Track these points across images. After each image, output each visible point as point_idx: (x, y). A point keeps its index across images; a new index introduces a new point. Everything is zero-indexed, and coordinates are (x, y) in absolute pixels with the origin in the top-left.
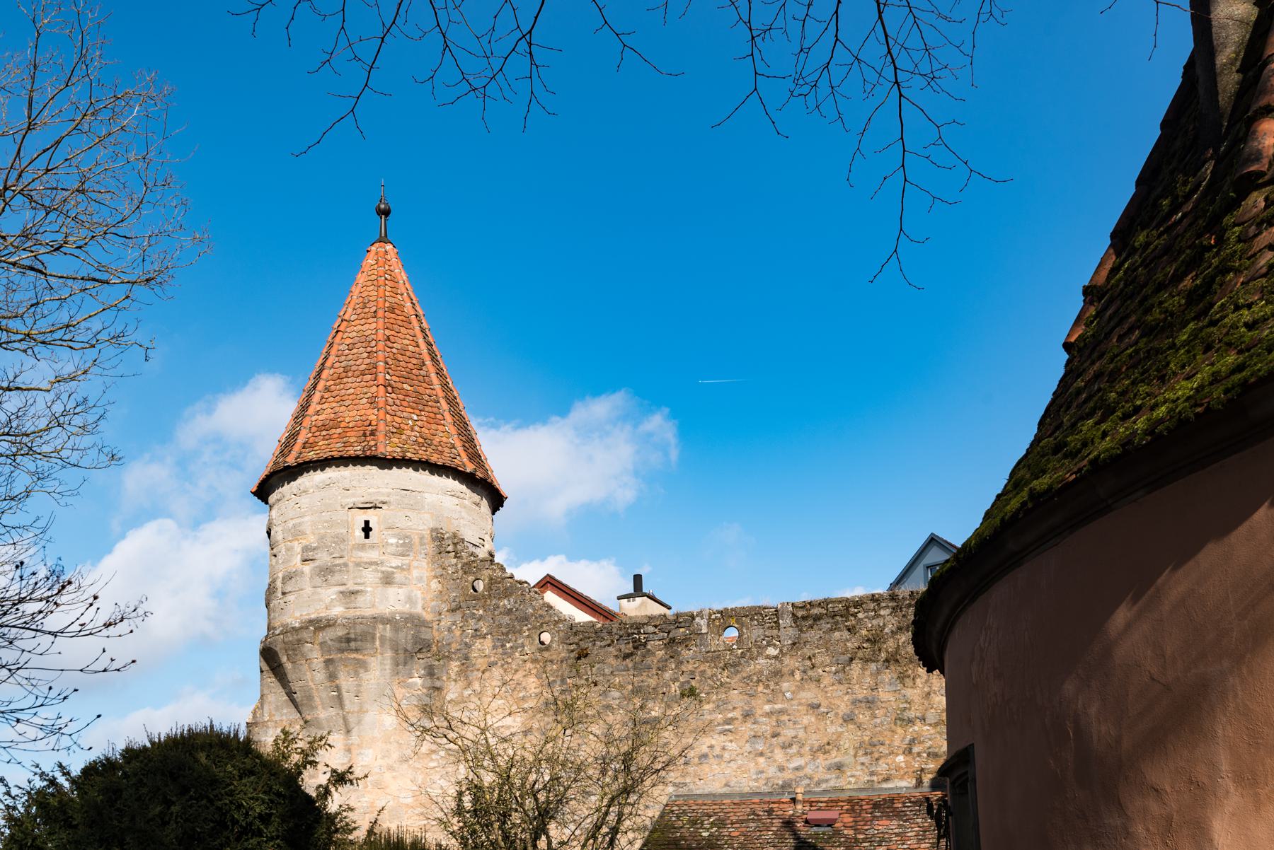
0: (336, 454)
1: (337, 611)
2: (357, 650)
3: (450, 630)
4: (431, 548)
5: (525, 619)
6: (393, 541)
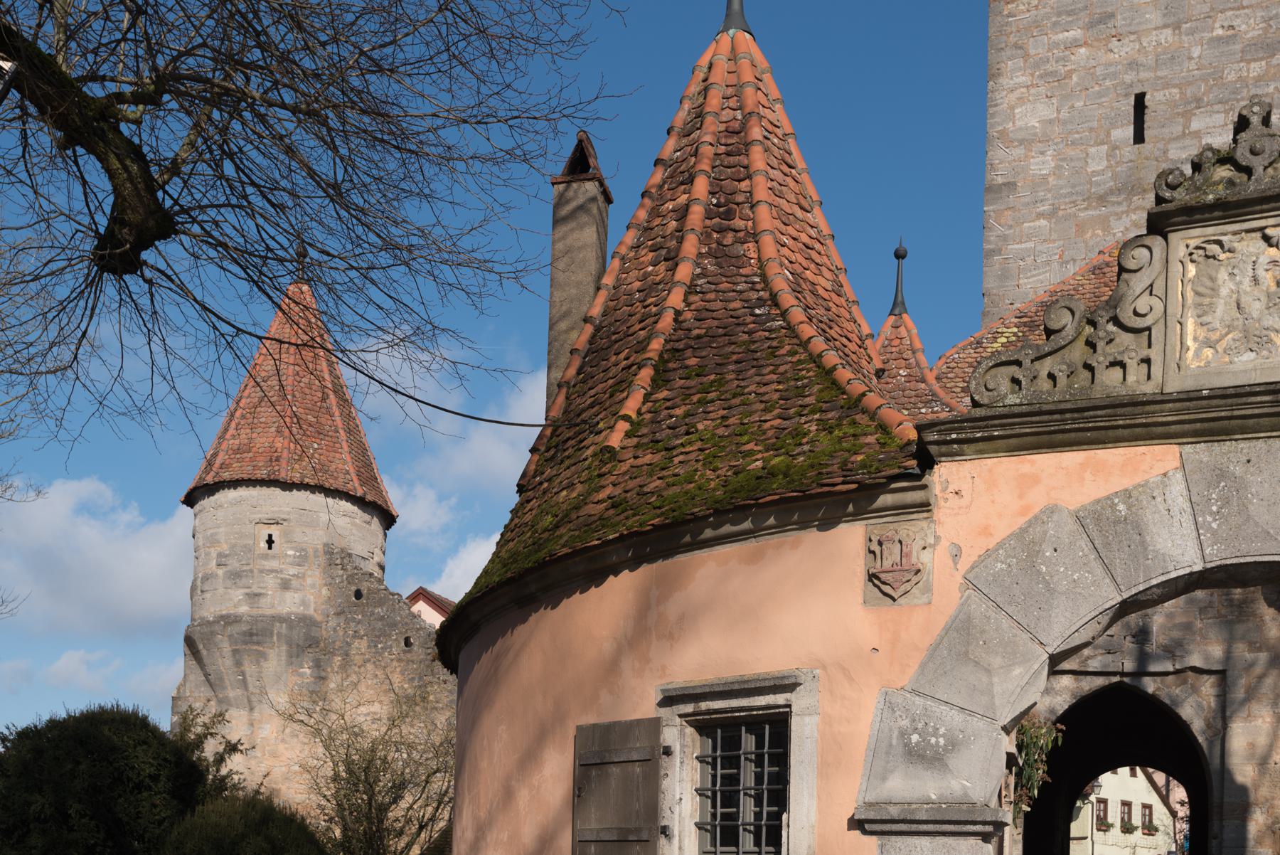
0: (245, 476)
1: (244, 609)
2: (258, 643)
3: (335, 630)
4: (323, 560)
5: (393, 625)
6: (291, 553)
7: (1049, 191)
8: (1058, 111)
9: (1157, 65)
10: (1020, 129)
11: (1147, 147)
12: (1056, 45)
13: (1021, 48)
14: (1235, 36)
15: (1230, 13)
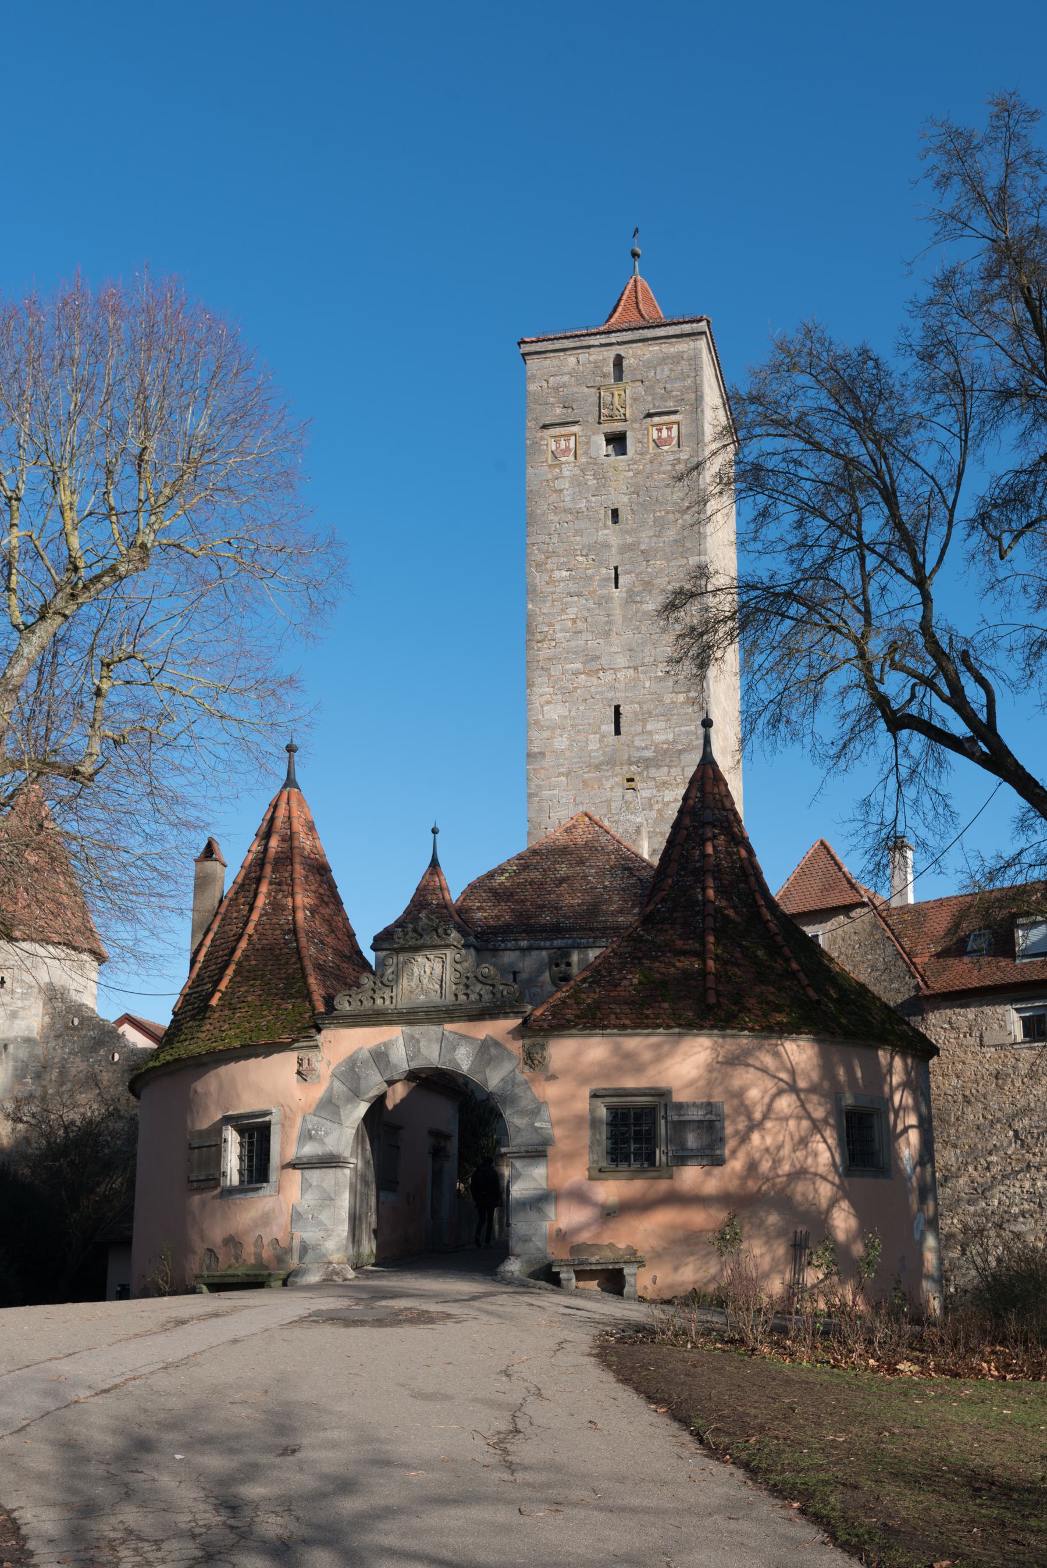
9: (626, 690)
11: (622, 737)
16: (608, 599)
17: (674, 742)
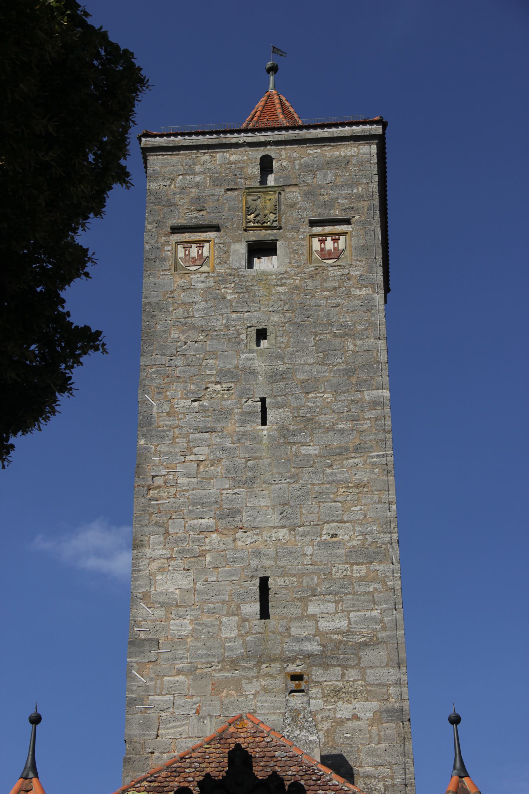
7: (188, 650)
8: (195, 584)
10: (161, 593)
11: (272, 622)
12: (193, 528)
13: (162, 526)
14: (339, 542)
15: (334, 525)
16: (255, 439)
17: (348, 633)
